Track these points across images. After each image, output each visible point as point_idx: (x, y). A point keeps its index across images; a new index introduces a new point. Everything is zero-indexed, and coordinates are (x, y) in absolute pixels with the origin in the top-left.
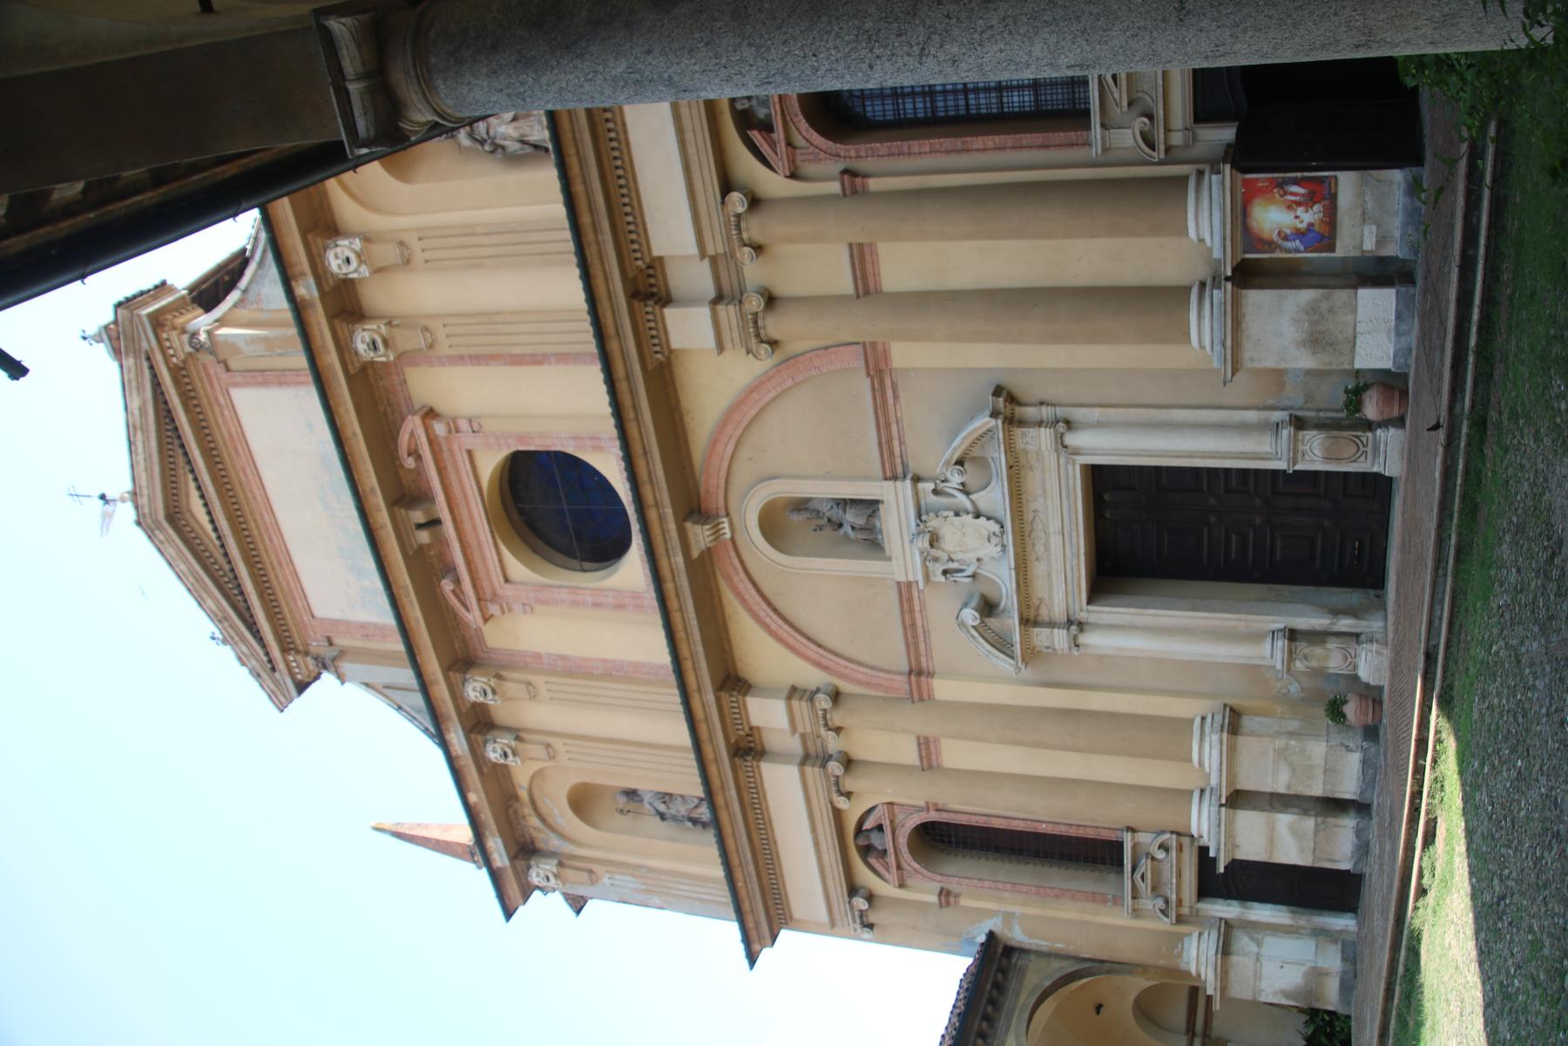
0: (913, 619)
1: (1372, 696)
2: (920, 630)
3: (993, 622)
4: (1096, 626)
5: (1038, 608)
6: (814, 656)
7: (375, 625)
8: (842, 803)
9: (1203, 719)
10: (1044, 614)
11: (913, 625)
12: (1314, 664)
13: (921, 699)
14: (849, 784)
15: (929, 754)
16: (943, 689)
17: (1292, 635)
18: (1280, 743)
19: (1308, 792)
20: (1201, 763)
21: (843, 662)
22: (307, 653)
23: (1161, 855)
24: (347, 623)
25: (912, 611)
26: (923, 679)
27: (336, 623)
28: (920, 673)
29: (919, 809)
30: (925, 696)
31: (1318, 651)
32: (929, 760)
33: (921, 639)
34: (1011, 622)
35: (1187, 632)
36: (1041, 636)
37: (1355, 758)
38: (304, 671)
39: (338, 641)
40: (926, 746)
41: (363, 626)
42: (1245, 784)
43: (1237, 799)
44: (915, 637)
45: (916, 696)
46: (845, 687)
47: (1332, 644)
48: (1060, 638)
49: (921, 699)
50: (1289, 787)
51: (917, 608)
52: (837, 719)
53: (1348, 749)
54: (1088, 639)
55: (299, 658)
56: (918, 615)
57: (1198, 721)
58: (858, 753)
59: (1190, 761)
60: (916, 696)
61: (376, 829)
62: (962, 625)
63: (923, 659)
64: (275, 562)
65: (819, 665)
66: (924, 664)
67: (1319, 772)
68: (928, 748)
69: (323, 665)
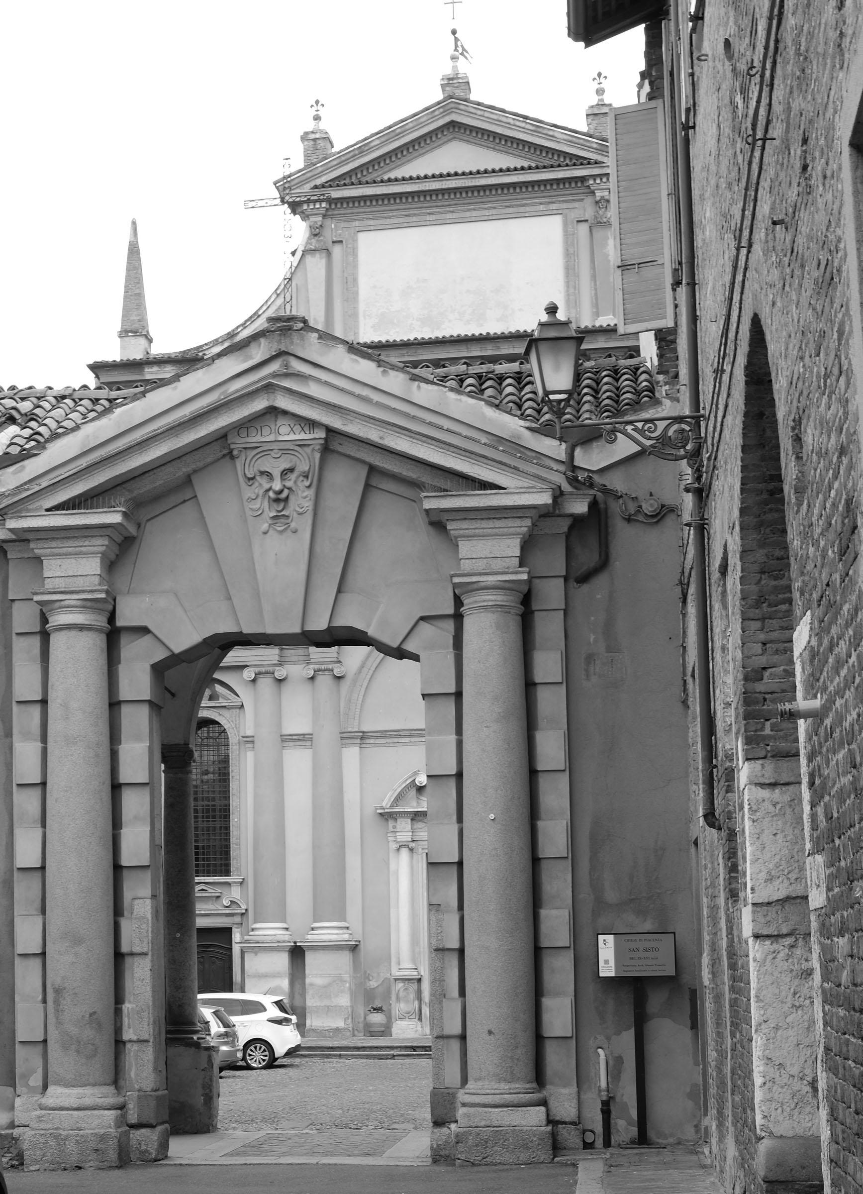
0: (405, 736)
1: (386, 1031)
2: (396, 740)
3: (413, 792)
4: (412, 858)
5: (420, 821)
6: (369, 663)
7: (357, 293)
8: (248, 674)
9: (348, 928)
10: (419, 825)
11: (400, 736)
12: (401, 994)
13: (342, 738)
14: (265, 683)
15: (294, 740)
16: (351, 755)
17: (419, 980)
18: (346, 977)
19: (308, 997)
20: (313, 929)
21: (365, 684)
22: (325, 216)
23: (226, 902)
24: (355, 266)
25: (411, 736)
26: (358, 741)
27: (354, 252)
28: (362, 738)
29: (237, 728)
30: (344, 741)
31: (412, 996)
32: (290, 740)
33: (388, 741)
34: (412, 806)
35: (414, 916)
36: (404, 825)
37: (340, 1024)
38: (309, 212)
39: (337, 251)
40: (304, 739)
41: (355, 280)
42: (309, 957)
43: (297, 953)
44: (391, 737)
45: (345, 735)
46: (345, 685)
47: (416, 1003)
48: (405, 836)
49: (342, 738)
50: (311, 985)
51: (413, 740)
52: (324, 680)
53: (345, 1020)
54: (404, 852)
55: (323, 211)
56: (407, 740)
57: (347, 925)
58: (287, 689)
59: (315, 921)
60: (345, 735)
61: (134, 223)
62: (416, 773)
63: (372, 741)
64: (411, 212)
65: (362, 666)
66: (368, 741)
67: (326, 1002)
68: (299, 740)
69: (316, 232)
